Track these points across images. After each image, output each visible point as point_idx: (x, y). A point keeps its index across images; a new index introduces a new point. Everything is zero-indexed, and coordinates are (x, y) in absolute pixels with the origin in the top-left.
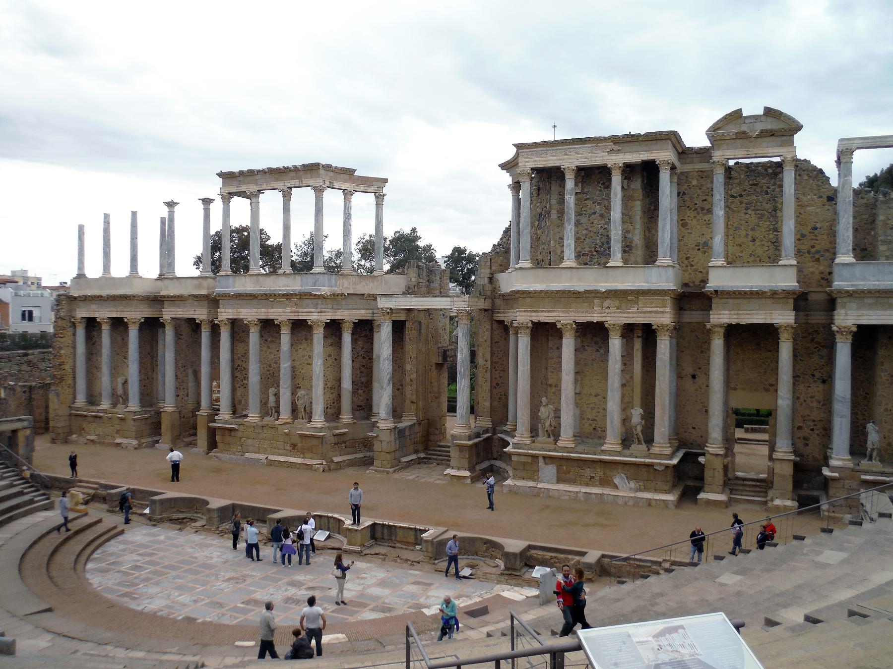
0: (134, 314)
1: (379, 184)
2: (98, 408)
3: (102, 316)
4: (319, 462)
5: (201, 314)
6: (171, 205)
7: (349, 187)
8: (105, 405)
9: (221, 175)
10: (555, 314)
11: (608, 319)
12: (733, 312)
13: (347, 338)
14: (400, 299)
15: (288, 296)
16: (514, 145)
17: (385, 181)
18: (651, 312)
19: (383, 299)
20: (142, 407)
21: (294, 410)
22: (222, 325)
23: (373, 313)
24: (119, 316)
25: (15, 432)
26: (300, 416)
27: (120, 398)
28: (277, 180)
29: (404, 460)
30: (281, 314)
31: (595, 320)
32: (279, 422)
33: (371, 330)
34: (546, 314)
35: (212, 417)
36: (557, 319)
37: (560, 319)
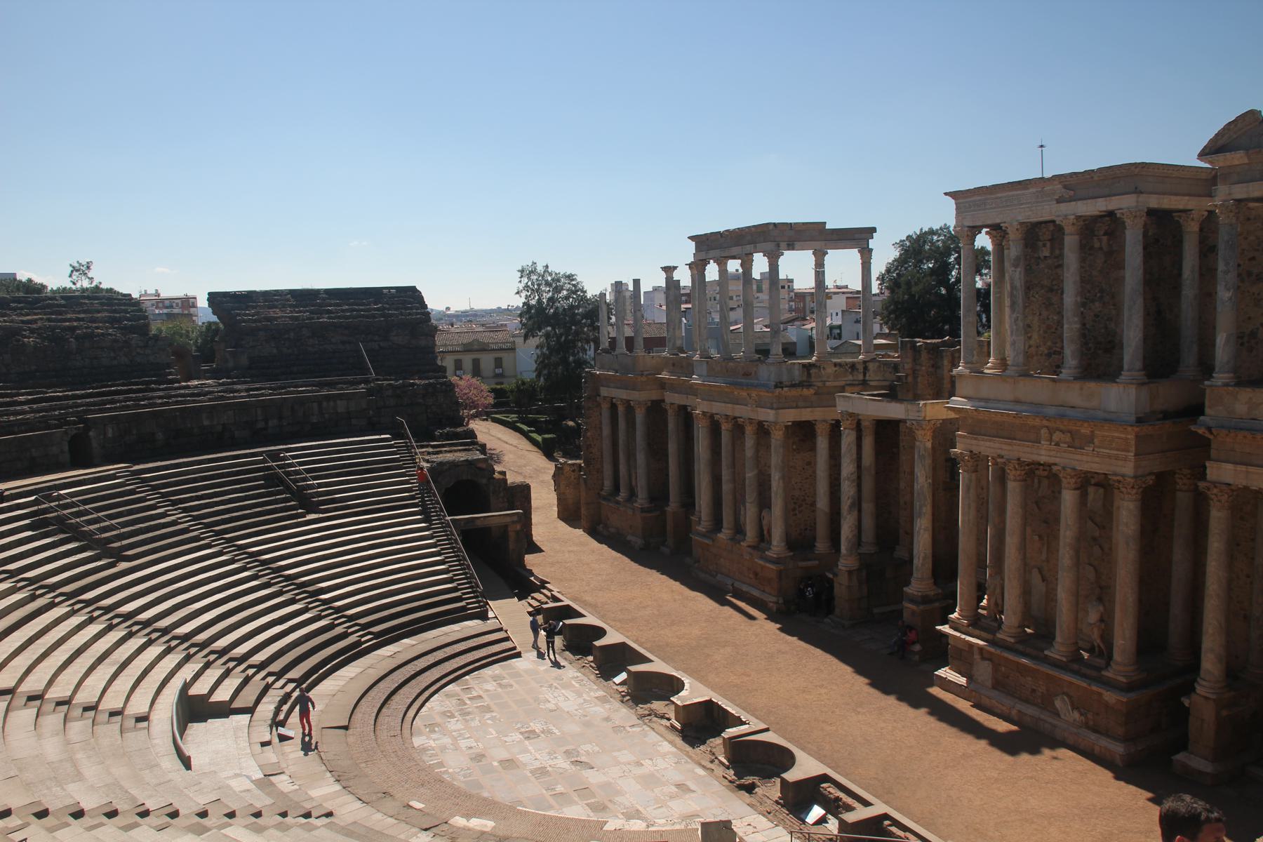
0: (641, 396)
1: (863, 236)
4: (774, 599)
6: (669, 270)
7: (818, 245)
9: (691, 238)
10: (997, 445)
11: (1057, 460)
12: (1240, 468)
13: (822, 444)
16: (946, 194)
17: (874, 230)
18: (1109, 457)
25: (506, 526)
29: (876, 611)
31: (1043, 459)
34: (988, 444)
36: (1000, 452)
37: (1003, 453)
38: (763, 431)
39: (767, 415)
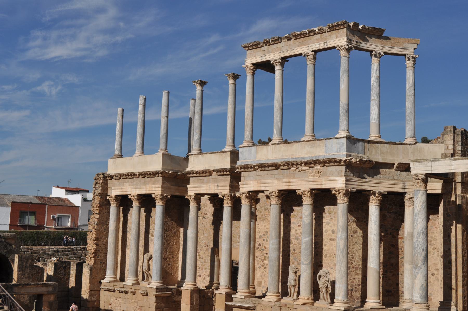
2: (124, 283)
3: (133, 193)
5: (222, 188)
8: (129, 280)
14: (437, 163)
15: (311, 163)
19: (417, 164)
20: (163, 283)
21: (315, 293)
22: (243, 197)
23: (404, 185)
24: (148, 192)
26: (321, 295)
27: (146, 277)
28: (300, 45)
30: (304, 183)
32: (300, 301)
33: (402, 206)
35: (229, 297)
38: (323, 198)
39: (337, 181)
